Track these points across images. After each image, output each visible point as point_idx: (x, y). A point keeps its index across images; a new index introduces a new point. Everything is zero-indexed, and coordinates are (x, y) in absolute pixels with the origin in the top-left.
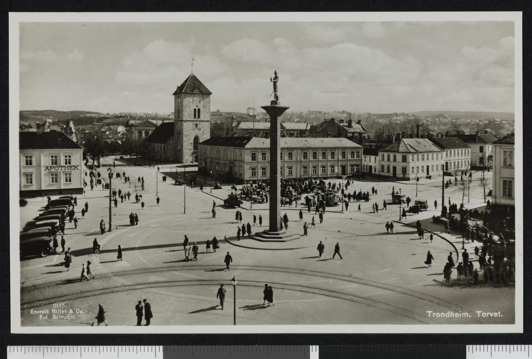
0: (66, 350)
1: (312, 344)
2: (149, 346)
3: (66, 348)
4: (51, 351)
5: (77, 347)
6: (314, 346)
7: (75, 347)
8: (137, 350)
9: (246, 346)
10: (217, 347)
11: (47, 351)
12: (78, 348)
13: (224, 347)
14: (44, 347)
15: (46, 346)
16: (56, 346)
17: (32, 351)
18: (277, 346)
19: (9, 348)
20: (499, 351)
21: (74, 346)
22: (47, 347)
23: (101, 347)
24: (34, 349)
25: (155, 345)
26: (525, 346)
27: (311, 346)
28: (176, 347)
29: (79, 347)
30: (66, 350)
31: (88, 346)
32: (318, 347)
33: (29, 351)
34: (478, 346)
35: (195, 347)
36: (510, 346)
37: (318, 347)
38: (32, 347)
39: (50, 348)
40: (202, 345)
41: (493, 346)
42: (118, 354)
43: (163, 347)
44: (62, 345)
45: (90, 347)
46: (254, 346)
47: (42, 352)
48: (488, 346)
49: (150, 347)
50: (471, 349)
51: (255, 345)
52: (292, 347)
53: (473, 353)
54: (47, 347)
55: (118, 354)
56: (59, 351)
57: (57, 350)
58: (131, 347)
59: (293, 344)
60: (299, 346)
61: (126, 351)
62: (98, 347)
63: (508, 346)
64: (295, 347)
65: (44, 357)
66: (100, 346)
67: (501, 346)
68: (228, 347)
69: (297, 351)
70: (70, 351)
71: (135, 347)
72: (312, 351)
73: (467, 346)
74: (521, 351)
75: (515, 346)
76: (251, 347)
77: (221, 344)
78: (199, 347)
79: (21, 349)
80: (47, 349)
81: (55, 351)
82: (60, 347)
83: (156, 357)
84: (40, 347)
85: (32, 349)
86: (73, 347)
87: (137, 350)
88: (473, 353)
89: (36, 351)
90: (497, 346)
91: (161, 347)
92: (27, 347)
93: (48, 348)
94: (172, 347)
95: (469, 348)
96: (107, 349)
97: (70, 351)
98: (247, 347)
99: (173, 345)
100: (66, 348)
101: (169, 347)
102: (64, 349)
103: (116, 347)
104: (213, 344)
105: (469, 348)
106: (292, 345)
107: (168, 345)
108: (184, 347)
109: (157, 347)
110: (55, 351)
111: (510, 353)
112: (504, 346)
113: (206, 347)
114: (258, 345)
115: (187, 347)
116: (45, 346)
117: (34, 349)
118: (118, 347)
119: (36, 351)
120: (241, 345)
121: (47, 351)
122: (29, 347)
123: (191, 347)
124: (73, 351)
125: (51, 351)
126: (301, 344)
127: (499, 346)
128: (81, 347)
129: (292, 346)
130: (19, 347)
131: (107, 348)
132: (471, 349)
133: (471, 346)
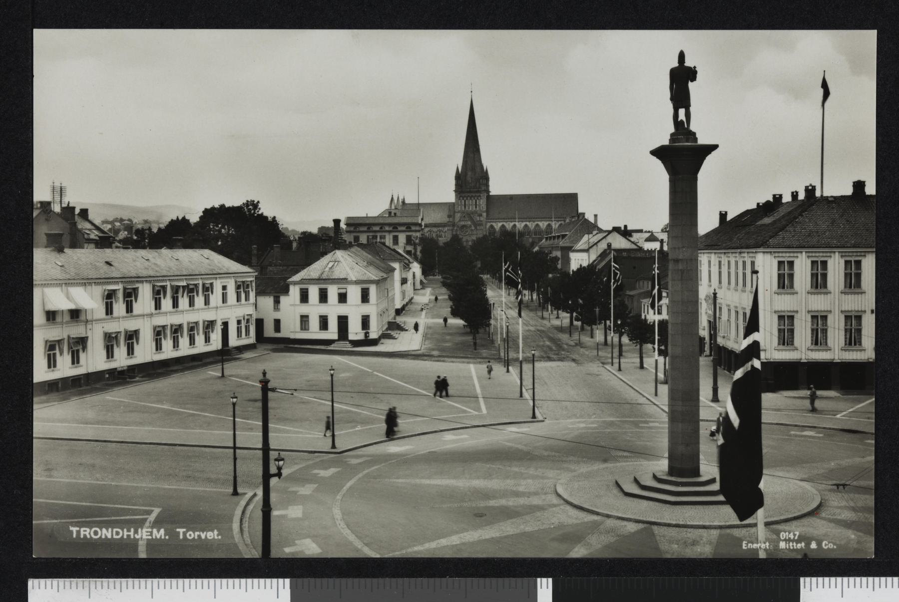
0: (127, 585)
1: (542, 576)
2: (267, 580)
3: (127, 583)
4: (102, 588)
6: (544, 580)
7: (143, 581)
9: (430, 579)
10: (381, 580)
12: (148, 582)
13: (394, 580)
14: (90, 581)
15: (95, 579)
16: (110, 580)
17: (71, 588)
18: (482, 580)
19: (30, 582)
20: (855, 587)
21: (141, 580)
22: (96, 581)
23: (187, 581)
24: (74, 585)
25: (277, 577)
27: (539, 580)
28: (312, 580)
29: (149, 581)
30: (127, 585)
32: (550, 580)
33: (64, 588)
34: (820, 579)
35: (344, 580)
36: (874, 579)
37: (550, 580)
38: (71, 581)
39: (100, 583)
40: (356, 577)
41: (845, 579)
42: (215, 593)
45: (168, 581)
46: (443, 579)
47: (87, 589)
48: (836, 579)
49: (268, 581)
50: (808, 585)
51: (445, 577)
52: (507, 580)
53: (811, 590)
54: (96, 581)
55: (215, 593)
56: (115, 588)
57: (111, 585)
58: (237, 581)
59: (509, 576)
60: (519, 580)
61: (227, 588)
62: (180, 581)
63: (871, 579)
66: (185, 580)
67: (858, 579)
68: (400, 580)
69: (516, 588)
70: (133, 588)
71: (243, 581)
72: (541, 588)
73: (802, 579)
75: (883, 579)
76: (438, 580)
77: (387, 576)
78: (350, 580)
79: (52, 584)
80: (96, 584)
81: (108, 588)
82: (118, 580)
83: (278, 597)
84: (83, 582)
85: (71, 584)
86: (140, 581)
88: (811, 590)
89: (77, 588)
90: (852, 579)
91: (287, 581)
92: (61, 581)
94: (306, 580)
95: (805, 582)
96: (196, 584)
97: (133, 588)
98: (431, 580)
99: (307, 577)
100: (127, 583)
101: (300, 580)
102: (124, 584)
103: (212, 581)
105: (805, 582)
108: (325, 580)
109: (281, 580)
110: (108, 588)
111: (874, 590)
112: (864, 579)
113: (362, 580)
114: (451, 577)
115: (331, 580)
116: (91, 579)
117: (74, 585)
118: (215, 581)
119: (77, 588)
120: (421, 577)
121: (96, 589)
122: (65, 581)
123: (338, 580)
125: (102, 588)
126: (522, 575)
128: (152, 581)
129: (507, 580)
130: (49, 581)
131: (196, 582)
132: (808, 585)
133: (808, 579)
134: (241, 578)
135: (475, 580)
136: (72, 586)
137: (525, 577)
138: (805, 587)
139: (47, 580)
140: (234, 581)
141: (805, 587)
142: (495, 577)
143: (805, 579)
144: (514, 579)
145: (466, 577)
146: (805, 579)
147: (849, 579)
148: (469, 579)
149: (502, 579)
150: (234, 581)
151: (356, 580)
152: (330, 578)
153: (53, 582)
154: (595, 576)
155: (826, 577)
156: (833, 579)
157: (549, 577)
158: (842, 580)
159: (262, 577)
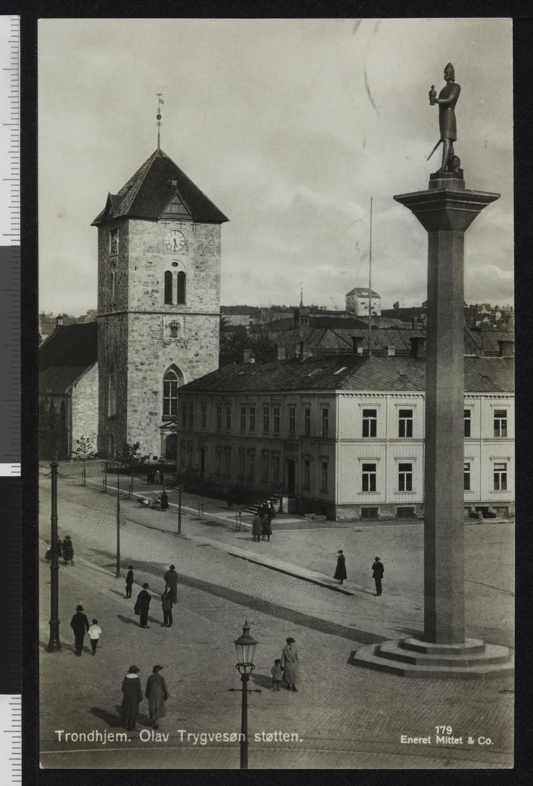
0: (15, 102)
5: (18, 119)
6: (19, 469)
8: (15, 207)
10: (19, 326)
11: (12, 75)
12: (17, 120)
13: (19, 337)
14: (18, 69)
16: (19, 87)
17: (12, 53)
18: (19, 414)
19: (16, 18)
21: (19, 115)
24: (15, 55)
25: (22, 235)
26: (20, 781)
27: (19, 464)
28: (19, 265)
29: (18, 122)
30: (15, 102)
31: (19, 134)
32: (19, 475)
33: (12, 47)
35: (19, 293)
37: (19, 475)
38: (18, 53)
39: (17, 79)
42: (7, 180)
43: (18, 246)
44: (21, 97)
50: (15, 701)
53: (10, 704)
55: (7, 180)
56: (12, 91)
57: (15, 89)
58: (18, 199)
59: (23, 438)
60: (19, 447)
61: (12, 191)
63: (20, 756)
64: (19, 442)
65: (4, 69)
68: (19, 342)
70: (12, 108)
73: (20, 696)
74: (13, 776)
76: (19, 376)
77: (23, 331)
78: (19, 298)
80: (16, 75)
82: (18, 94)
83: (4, 235)
84: (18, 64)
85: (16, 53)
86: (18, 113)
87: (15, 207)
88: (10, 704)
91: (18, 243)
92: (18, 44)
93: (16, 76)
94: (19, 260)
95: (17, 698)
97: (12, 108)
98: (19, 370)
99: (21, 260)
101: (19, 254)
104: (22, 319)
105: (17, 698)
106: (22, 437)
107: (22, 253)
108: (19, 276)
109: (19, 238)
111: (10, 759)
115: (19, 282)
116: (20, 70)
117: (15, 55)
120: (22, 361)
121: (12, 75)
123: (19, 287)
124: (12, 113)
126: (23, 450)
127: (19, 743)
129: (19, 436)
131: (17, 163)
132: (15, 701)
133: (20, 701)
134: (21, 186)
135: (19, 409)
136: (14, 54)
137: (22, 453)
138: (13, 698)
139: (19, 32)
140: (18, 196)
141: (13, 698)
142: (22, 426)
143: (19, 698)
144: (20, 443)
145: (22, 400)
146: (19, 698)
147: (19, 732)
148: (20, 403)
149: (20, 432)
150: (18, 196)
151: (19, 304)
152: (21, 281)
153: (17, 38)
154: (22, 513)
155: (22, 717)
156: (20, 723)
157: (21, 474)
158: (19, 732)
159: (21, 221)
